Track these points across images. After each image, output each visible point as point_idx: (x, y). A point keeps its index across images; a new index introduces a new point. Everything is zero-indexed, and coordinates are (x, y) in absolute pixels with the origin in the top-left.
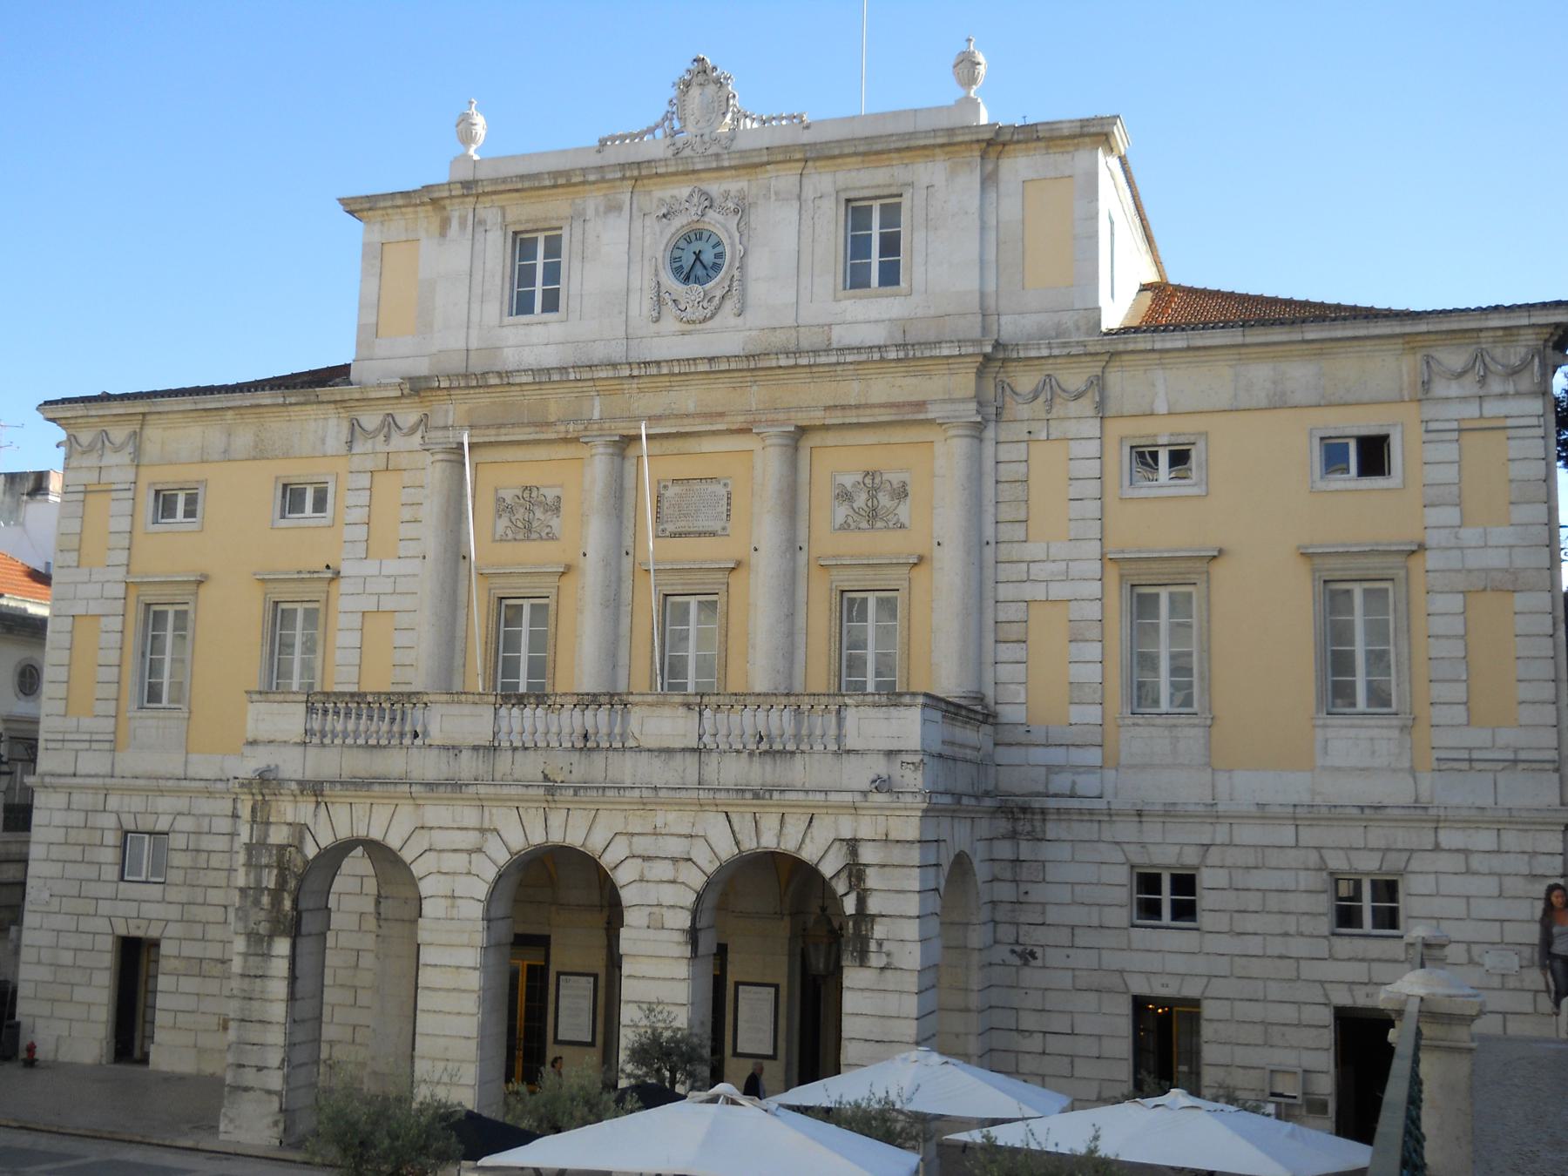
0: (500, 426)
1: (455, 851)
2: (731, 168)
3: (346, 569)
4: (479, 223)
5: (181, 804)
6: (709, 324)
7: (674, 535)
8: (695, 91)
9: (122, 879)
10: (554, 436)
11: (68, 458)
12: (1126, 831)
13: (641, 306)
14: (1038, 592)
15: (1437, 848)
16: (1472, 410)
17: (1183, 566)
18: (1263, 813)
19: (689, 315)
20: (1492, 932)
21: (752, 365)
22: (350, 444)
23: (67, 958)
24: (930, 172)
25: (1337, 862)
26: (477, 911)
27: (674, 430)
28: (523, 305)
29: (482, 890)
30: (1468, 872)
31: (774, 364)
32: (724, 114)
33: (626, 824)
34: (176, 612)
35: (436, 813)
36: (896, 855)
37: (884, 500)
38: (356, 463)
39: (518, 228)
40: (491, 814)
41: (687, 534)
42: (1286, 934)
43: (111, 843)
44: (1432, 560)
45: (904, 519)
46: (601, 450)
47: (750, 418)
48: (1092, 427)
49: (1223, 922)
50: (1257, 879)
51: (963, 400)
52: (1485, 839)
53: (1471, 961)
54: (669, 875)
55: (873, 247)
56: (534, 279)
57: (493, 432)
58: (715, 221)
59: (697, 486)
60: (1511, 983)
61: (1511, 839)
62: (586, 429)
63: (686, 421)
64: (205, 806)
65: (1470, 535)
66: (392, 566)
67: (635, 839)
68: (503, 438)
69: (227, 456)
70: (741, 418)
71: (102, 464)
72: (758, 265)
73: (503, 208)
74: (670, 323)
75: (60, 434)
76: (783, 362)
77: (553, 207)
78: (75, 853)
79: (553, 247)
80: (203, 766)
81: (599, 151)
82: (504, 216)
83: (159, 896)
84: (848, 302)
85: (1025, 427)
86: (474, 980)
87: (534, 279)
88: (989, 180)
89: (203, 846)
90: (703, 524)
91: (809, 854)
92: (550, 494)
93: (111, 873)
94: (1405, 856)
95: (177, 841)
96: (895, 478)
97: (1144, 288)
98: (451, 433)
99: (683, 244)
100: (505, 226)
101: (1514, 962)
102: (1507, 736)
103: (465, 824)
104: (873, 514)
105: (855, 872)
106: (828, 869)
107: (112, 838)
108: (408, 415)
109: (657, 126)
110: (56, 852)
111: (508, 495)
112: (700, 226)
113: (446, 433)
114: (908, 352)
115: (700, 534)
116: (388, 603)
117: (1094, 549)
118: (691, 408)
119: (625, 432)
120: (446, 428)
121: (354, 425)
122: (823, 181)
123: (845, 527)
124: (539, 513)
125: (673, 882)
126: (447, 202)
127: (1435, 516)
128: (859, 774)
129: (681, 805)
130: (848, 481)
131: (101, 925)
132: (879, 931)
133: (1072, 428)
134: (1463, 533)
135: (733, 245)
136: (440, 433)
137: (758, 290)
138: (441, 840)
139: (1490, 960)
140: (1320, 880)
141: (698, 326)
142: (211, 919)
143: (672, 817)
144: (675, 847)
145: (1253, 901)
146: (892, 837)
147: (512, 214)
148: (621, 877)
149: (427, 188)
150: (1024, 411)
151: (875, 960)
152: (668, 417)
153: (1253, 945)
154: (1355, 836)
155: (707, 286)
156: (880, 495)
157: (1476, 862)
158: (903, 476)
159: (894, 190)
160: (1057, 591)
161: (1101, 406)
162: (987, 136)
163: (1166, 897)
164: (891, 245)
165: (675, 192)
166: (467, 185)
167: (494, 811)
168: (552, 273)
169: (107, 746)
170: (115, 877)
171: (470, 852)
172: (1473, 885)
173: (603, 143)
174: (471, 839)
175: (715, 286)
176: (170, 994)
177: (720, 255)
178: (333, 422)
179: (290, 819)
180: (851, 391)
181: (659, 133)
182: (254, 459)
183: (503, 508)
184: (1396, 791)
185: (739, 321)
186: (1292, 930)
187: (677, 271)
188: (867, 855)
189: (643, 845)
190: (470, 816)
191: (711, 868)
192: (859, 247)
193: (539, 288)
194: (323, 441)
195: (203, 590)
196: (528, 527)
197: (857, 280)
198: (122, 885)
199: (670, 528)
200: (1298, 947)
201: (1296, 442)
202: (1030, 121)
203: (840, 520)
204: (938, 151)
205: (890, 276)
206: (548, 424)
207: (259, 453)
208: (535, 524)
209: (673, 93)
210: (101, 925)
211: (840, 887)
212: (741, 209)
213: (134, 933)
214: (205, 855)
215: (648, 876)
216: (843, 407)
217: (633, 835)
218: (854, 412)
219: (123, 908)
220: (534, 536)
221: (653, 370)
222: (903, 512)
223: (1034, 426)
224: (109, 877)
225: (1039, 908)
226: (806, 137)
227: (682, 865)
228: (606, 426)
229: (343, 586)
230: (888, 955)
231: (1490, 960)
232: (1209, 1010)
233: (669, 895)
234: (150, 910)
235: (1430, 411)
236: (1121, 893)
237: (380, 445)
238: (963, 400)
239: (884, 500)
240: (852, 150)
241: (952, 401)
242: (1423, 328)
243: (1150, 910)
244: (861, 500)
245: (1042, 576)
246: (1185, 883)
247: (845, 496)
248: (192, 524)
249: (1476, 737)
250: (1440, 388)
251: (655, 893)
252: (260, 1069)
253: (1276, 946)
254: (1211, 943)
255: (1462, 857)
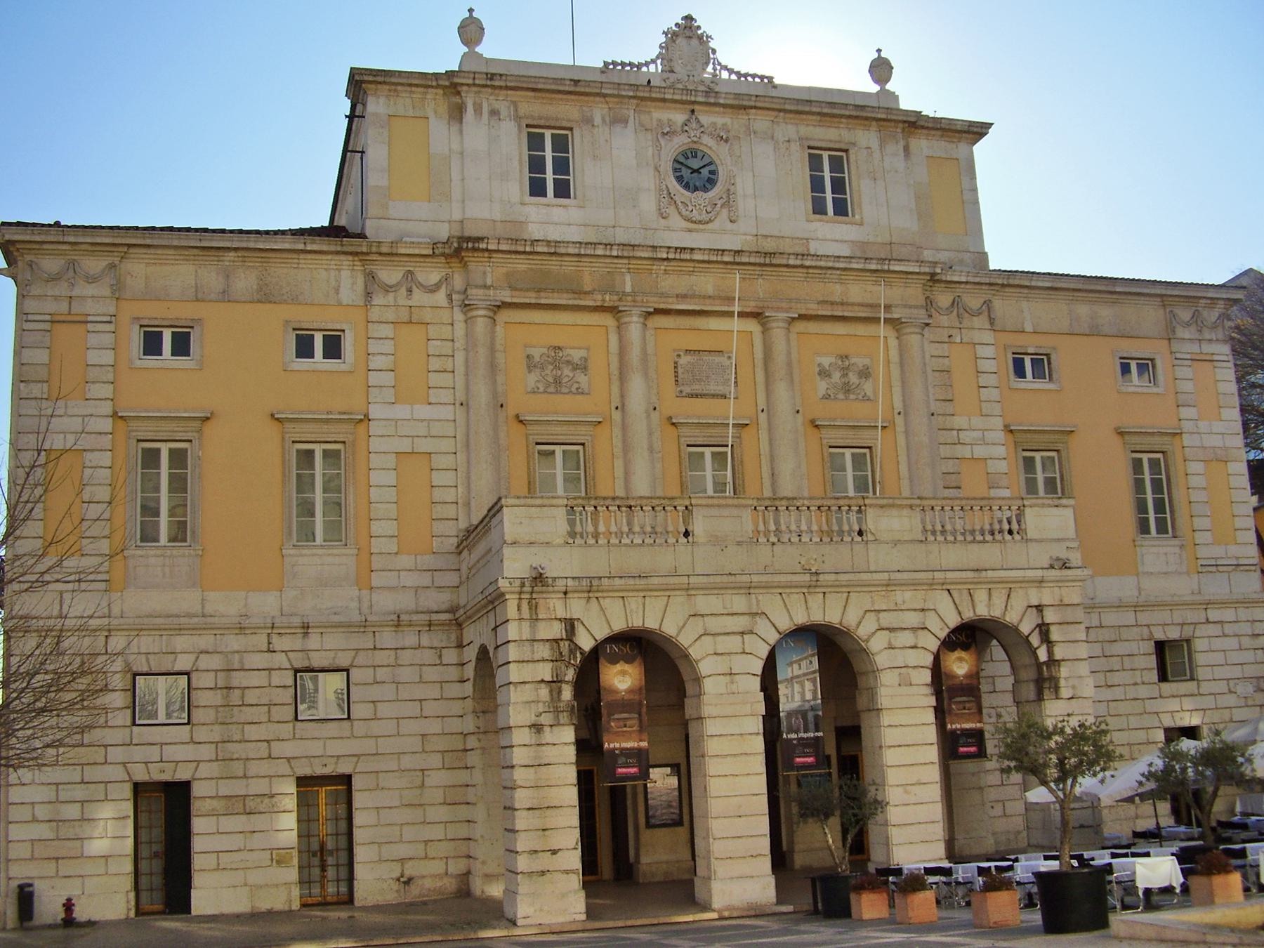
0: (539, 291)
1: (728, 634)
2: (724, 106)
3: (375, 411)
4: (494, 113)
5: (205, 641)
6: (710, 226)
7: (692, 396)
8: (681, 41)
9: (134, 724)
10: (591, 303)
13: (648, 204)
14: (965, 452)
15: (1208, 621)
16: (1195, 348)
17: (1052, 437)
18: (1120, 606)
19: (696, 215)
20: (1237, 672)
21: (768, 261)
22: (368, 294)
24: (866, 138)
25: (1160, 636)
27: (697, 308)
28: (537, 189)
31: (784, 262)
32: (707, 64)
34: (171, 451)
35: (705, 603)
36: (1070, 615)
37: (853, 378)
38: (375, 314)
39: (530, 122)
40: (758, 601)
41: (702, 396)
42: (1136, 684)
43: (120, 686)
44: (1186, 440)
45: (870, 393)
46: (635, 319)
47: (761, 304)
48: (988, 337)
50: (1119, 648)
51: (916, 307)
52: (1229, 615)
53: (1230, 692)
54: (911, 642)
55: (831, 190)
56: (549, 172)
57: (533, 294)
58: (708, 144)
59: (706, 357)
60: (1250, 703)
61: (1243, 614)
62: (620, 300)
63: (708, 301)
64: (234, 642)
65: (1203, 426)
66: (423, 411)
67: (882, 615)
68: (543, 301)
69: (226, 296)
70: (753, 304)
71: (73, 294)
72: (744, 185)
73: (515, 103)
74: (676, 221)
76: (791, 262)
77: (566, 110)
79: (561, 144)
80: (224, 605)
81: (603, 72)
82: (516, 110)
83: (187, 738)
84: (818, 224)
85: (946, 333)
87: (549, 172)
88: (906, 149)
89: (235, 683)
90: (713, 388)
91: (1011, 618)
92: (576, 355)
93: (124, 718)
94: (1192, 627)
95: (201, 680)
96: (860, 362)
98: (492, 292)
100: (518, 118)
101: (1250, 689)
102: (1233, 550)
103: (735, 610)
104: (847, 389)
105: (1044, 630)
106: (1025, 628)
107: (118, 681)
108: (431, 275)
109: (653, 61)
111: (536, 353)
112: (695, 146)
113: (487, 292)
114: (877, 264)
115: (713, 396)
116: (424, 446)
117: (998, 423)
118: (710, 290)
119: (656, 306)
120: (485, 287)
121: (371, 277)
122: (788, 130)
123: (827, 397)
125: (914, 647)
126: (465, 88)
127: (1185, 412)
128: (1041, 555)
129: (914, 585)
130: (826, 361)
131: (118, 773)
132: (1064, 671)
133: (978, 336)
134: (1201, 424)
136: (481, 292)
137: (745, 205)
138: (714, 624)
139: (1239, 689)
140: (1150, 646)
141: (701, 226)
142: (251, 755)
143: (908, 595)
144: (912, 619)
145: (1115, 663)
146: (1066, 601)
147: (524, 108)
148: (876, 644)
149: (450, 74)
150: (944, 320)
151: (1064, 693)
152: (693, 296)
153: (1118, 693)
154: (1164, 616)
155: (711, 194)
156: (851, 374)
157: (1228, 629)
158: (867, 361)
159: (843, 146)
160: (980, 451)
161: (992, 321)
162: (913, 119)
164: (838, 186)
165: (671, 116)
166: (492, 76)
167: (760, 597)
168: (562, 166)
169: (102, 586)
170: (129, 723)
171: (743, 633)
174: (741, 623)
176: (208, 835)
178: (345, 274)
179: (561, 614)
180: (836, 291)
181: (652, 68)
182: (259, 301)
183: (531, 365)
184: (1182, 587)
185: (734, 226)
186: (1139, 681)
187: (680, 179)
188: (1050, 616)
189: (886, 619)
190: (739, 603)
191: (943, 634)
193: (550, 176)
194: (337, 291)
195: (208, 428)
196: (558, 381)
197: (819, 208)
198: (135, 728)
199: (687, 390)
200: (1143, 692)
201: (1105, 356)
202: (938, 115)
203: (822, 392)
204: (874, 123)
205: (841, 209)
206: (586, 293)
207: (265, 296)
208: (566, 380)
210: (118, 773)
211: (1035, 640)
214: (238, 692)
215: (897, 643)
216: (832, 303)
217: (879, 611)
218: (840, 308)
219: (138, 753)
220: (564, 390)
221: (686, 256)
222: (868, 387)
223: (952, 332)
224: (119, 722)
225: (990, 680)
226: (774, 93)
227: (920, 632)
228: (639, 299)
229: (374, 428)
230: (1074, 687)
231: (1241, 689)
233: (914, 658)
234: (171, 752)
235: (1176, 346)
237: (402, 301)
238: (916, 307)
239: (853, 378)
240: (818, 110)
241: (910, 307)
242: (1176, 293)
244: (836, 376)
245: (967, 440)
247: (824, 373)
248: (181, 362)
249: (1218, 551)
250: (1182, 333)
251: (901, 658)
252: (554, 852)
253: (1131, 692)
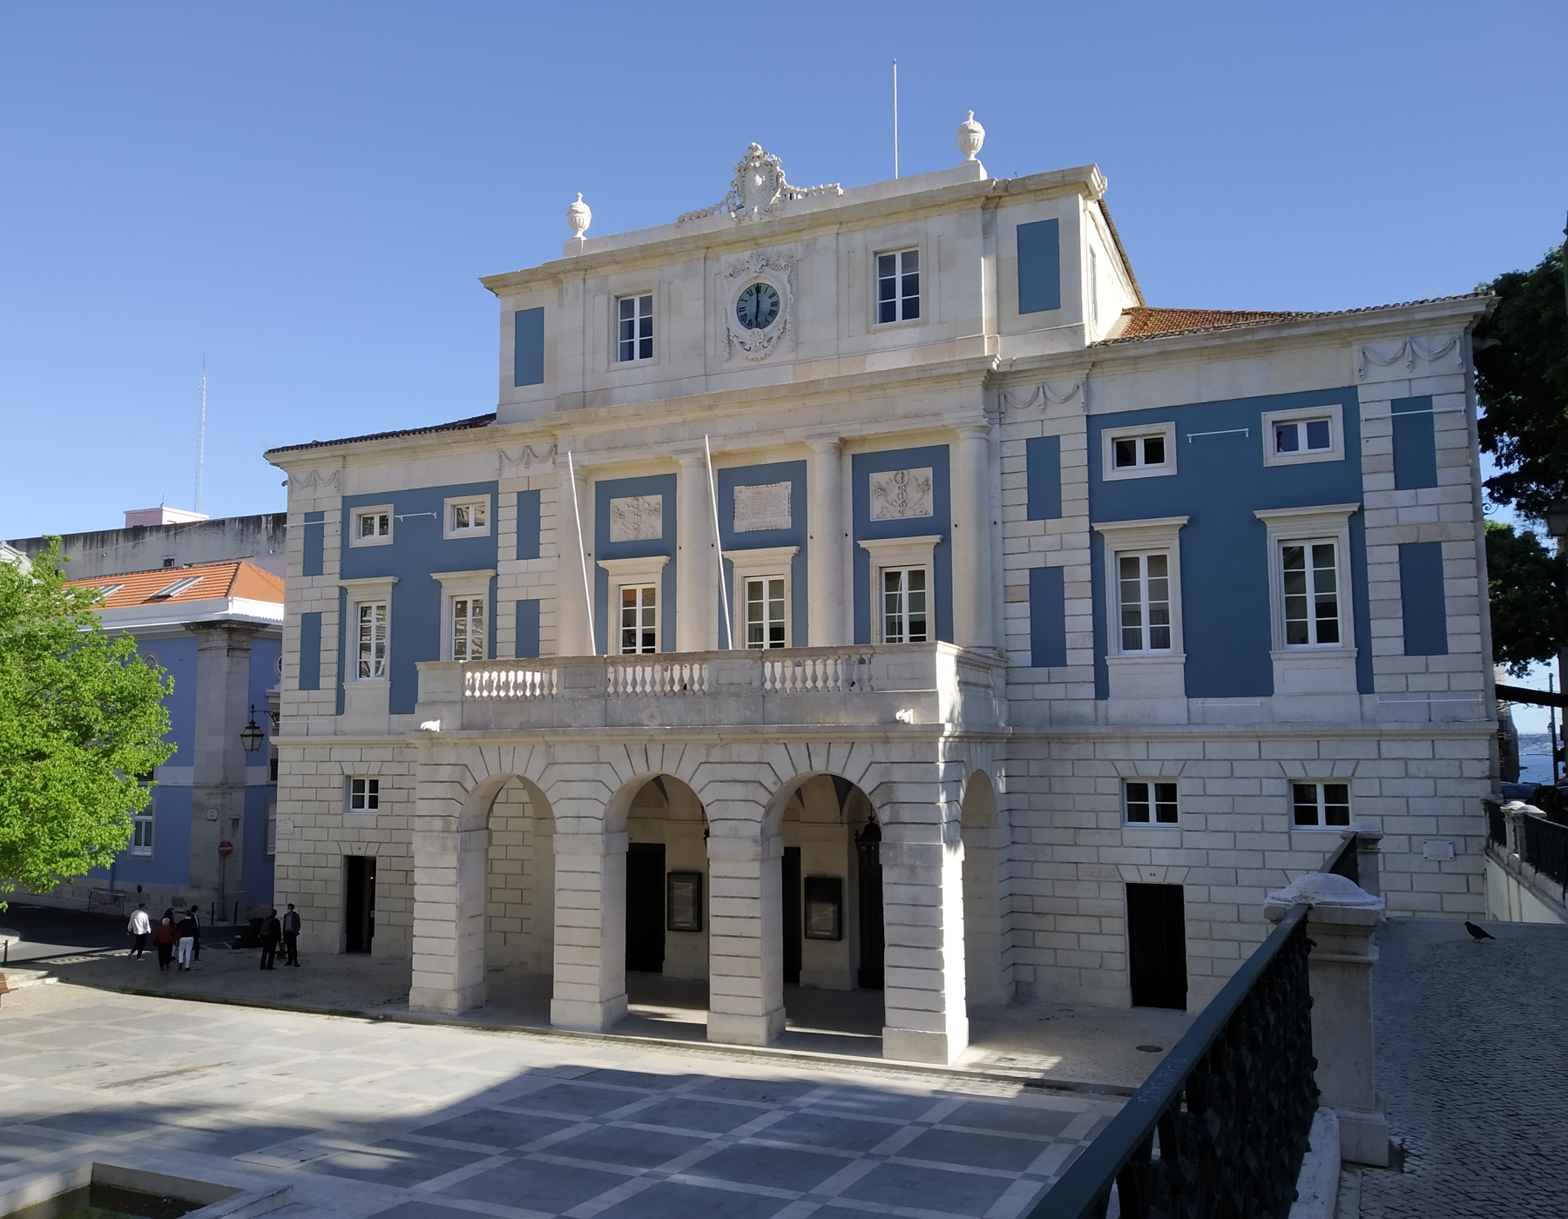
11: (290, 493)
12: (1115, 751)
20: (1429, 826)
23: (308, 873)
25: (1296, 772)
26: (598, 826)
29: (600, 811)
30: (1407, 776)
33: (708, 755)
49: (1198, 822)
75: (285, 476)
78: (310, 794)
86: (595, 882)
97: (1126, 312)
99: (746, 297)
110: (296, 794)
124: (645, 517)
135: (785, 294)
144: (745, 772)
157: (1413, 768)
163: (1152, 803)
172: (1412, 787)
173: (682, 221)
175: (772, 329)
177: (776, 304)
187: (743, 318)
192: (887, 289)
193: (637, 339)
209: (735, 175)
210: (334, 848)
212: (793, 265)
213: (356, 853)
231: (1427, 849)
232: (1189, 894)
234: (369, 835)
236: (1114, 801)
243: (1139, 814)
246: (1167, 791)
254: (1191, 840)
255: (1402, 763)
